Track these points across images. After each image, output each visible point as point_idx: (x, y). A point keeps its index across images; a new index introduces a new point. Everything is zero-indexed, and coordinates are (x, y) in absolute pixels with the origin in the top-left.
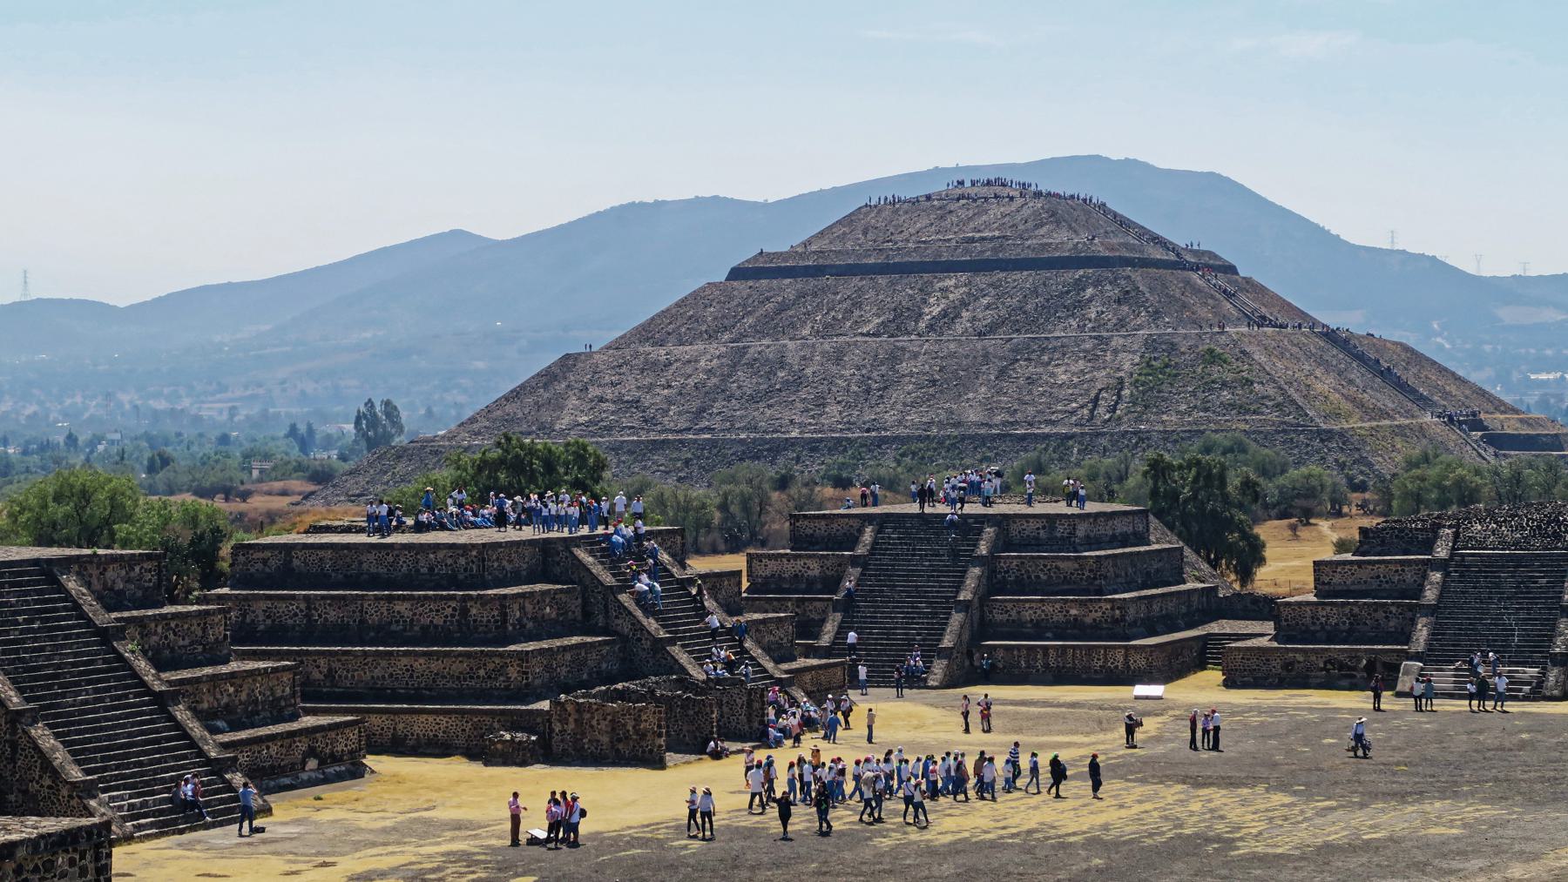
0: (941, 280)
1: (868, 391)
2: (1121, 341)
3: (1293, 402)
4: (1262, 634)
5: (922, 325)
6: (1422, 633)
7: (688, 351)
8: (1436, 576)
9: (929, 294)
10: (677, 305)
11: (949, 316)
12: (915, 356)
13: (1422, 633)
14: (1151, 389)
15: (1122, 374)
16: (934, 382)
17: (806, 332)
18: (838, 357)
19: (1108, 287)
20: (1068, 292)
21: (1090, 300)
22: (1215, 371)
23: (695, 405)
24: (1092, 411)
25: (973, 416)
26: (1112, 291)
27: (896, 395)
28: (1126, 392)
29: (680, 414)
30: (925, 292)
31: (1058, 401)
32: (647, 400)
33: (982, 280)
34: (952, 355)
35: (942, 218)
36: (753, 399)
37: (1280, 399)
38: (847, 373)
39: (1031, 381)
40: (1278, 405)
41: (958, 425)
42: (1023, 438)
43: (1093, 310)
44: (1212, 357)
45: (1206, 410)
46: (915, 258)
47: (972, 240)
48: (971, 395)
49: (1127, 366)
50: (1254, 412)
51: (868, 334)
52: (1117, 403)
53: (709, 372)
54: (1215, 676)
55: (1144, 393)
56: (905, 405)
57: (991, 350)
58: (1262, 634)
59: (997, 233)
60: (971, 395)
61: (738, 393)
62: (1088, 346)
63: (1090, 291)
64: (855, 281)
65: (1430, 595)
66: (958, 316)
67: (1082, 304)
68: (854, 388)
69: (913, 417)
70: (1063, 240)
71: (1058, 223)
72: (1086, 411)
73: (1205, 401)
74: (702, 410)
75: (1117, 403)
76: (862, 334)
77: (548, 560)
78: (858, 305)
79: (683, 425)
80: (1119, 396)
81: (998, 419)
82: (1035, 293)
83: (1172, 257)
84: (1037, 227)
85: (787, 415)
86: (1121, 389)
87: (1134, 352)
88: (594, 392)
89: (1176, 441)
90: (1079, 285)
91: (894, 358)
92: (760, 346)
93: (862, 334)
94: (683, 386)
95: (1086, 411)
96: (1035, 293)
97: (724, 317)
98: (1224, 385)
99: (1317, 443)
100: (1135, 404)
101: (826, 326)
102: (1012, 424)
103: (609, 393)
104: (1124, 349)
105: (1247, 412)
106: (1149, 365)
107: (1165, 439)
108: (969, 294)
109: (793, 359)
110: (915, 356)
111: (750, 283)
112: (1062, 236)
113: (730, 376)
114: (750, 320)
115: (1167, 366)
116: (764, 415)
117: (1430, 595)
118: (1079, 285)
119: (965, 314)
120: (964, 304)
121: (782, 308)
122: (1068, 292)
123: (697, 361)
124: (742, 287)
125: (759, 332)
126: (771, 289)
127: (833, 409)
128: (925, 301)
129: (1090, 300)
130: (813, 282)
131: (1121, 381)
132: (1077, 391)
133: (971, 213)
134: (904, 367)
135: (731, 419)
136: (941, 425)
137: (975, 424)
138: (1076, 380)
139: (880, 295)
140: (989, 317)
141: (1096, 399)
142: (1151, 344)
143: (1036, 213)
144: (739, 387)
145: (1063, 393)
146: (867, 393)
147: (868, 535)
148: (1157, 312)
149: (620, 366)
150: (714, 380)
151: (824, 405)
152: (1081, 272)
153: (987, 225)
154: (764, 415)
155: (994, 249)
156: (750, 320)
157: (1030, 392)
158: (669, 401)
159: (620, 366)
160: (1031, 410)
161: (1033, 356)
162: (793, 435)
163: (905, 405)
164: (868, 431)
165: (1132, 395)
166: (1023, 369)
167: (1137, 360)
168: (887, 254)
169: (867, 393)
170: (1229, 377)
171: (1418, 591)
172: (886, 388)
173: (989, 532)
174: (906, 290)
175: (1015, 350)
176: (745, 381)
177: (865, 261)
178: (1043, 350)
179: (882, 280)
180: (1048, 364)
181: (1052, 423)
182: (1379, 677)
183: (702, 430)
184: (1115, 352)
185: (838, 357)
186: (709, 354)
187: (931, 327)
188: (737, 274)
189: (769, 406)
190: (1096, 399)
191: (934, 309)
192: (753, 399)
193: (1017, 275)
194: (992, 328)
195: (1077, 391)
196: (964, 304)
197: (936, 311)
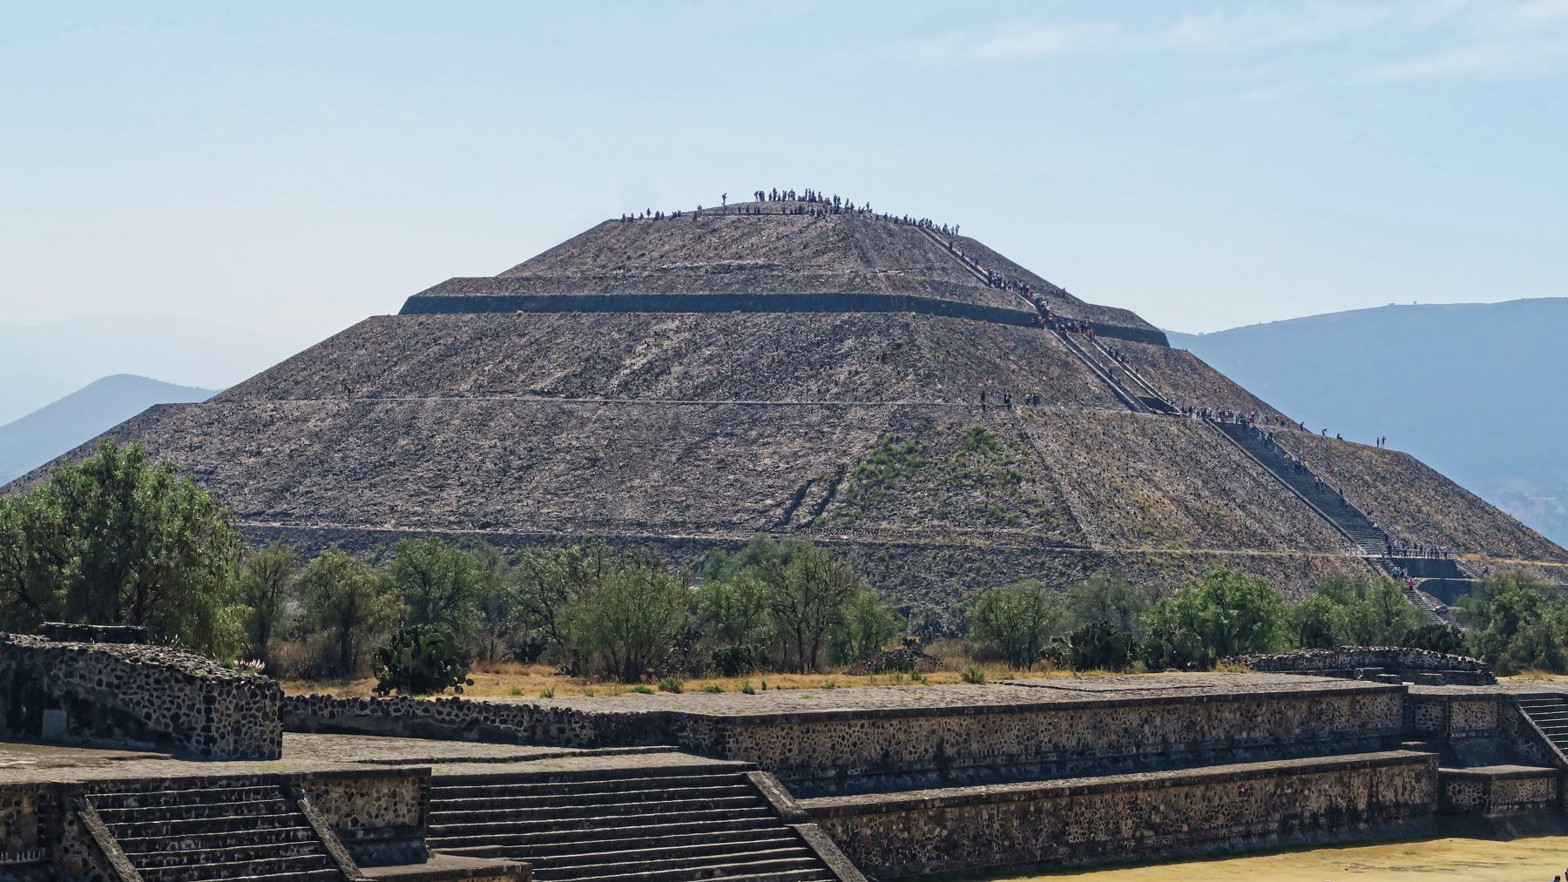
0: (661, 320)
1: (504, 471)
2: (861, 413)
3: (1067, 510)
9: (638, 340)
10: (324, 345)
11: (653, 372)
12: (583, 423)
14: (879, 483)
15: (846, 460)
16: (594, 461)
17: (465, 386)
18: (481, 423)
19: (876, 338)
20: (818, 344)
21: (845, 355)
22: (977, 463)
23: (282, 479)
24: (788, 512)
26: (878, 344)
27: (540, 478)
28: (844, 486)
29: (257, 491)
31: (749, 494)
32: (225, 470)
33: (713, 323)
34: (633, 424)
35: (700, 239)
36: (355, 476)
37: (1050, 506)
38: (486, 444)
39: (722, 465)
40: (1047, 515)
41: (608, 522)
42: (680, 544)
43: (846, 368)
44: (980, 440)
45: (944, 516)
46: (641, 291)
47: (727, 269)
48: (637, 482)
49: (856, 450)
50: (1010, 523)
51: (541, 393)
52: (826, 501)
53: (316, 435)
55: (867, 488)
56: (546, 491)
57: (685, 420)
59: (760, 262)
60: (637, 482)
61: (339, 466)
62: (814, 419)
63: (849, 343)
64: (553, 319)
66: (666, 371)
67: (832, 361)
68: (489, 466)
69: (553, 510)
70: (843, 271)
71: (846, 249)
72: (779, 511)
73: (946, 504)
74: (286, 488)
75: (826, 501)
76: (535, 393)
78: (543, 352)
79: (252, 508)
80: (832, 492)
81: (659, 518)
82: (777, 344)
83: (1029, 307)
84: (817, 253)
85: (391, 499)
86: (839, 481)
87: (873, 430)
89: (882, 560)
90: (838, 334)
91: (554, 425)
92: (395, 406)
93: (535, 393)
94: (276, 453)
95: (779, 511)
97: (373, 363)
98: (981, 480)
99: (1076, 572)
100: (850, 504)
101: (495, 379)
102: (674, 524)
104: (863, 425)
105: (999, 521)
106: (887, 449)
107: (869, 556)
108: (689, 342)
109: (424, 423)
110: (583, 423)
111: (423, 318)
112: (847, 268)
113: (338, 442)
114: (403, 368)
115: (910, 451)
116: (356, 499)
118: (838, 334)
119: (677, 369)
120: (678, 355)
121: (452, 351)
122: (818, 344)
123: (306, 420)
124: (412, 321)
125: (407, 384)
126: (446, 326)
127: (452, 494)
128: (629, 350)
129: (845, 355)
130: (500, 318)
131: (842, 470)
132: (779, 482)
133: (738, 234)
134: (562, 439)
135: (317, 502)
136: (582, 523)
137: (631, 524)
138: (782, 466)
139: (575, 336)
140: (703, 374)
141: (801, 493)
142: (898, 421)
143: (823, 236)
144: (343, 459)
145: (758, 485)
146: (508, 472)
148: (928, 376)
149: (210, 424)
150: (317, 447)
151: (442, 488)
152: (845, 316)
153: (753, 250)
154: (356, 499)
155: (746, 282)
156: (403, 368)
157: (716, 482)
158: (251, 474)
159: (210, 424)
160: (709, 507)
161: (739, 430)
162: (387, 527)
163: (546, 491)
164: (484, 526)
165: (850, 490)
166: (722, 447)
167: (873, 440)
168: (609, 285)
169: (508, 472)
170: (988, 469)
172: (530, 467)
174: (614, 329)
175: (718, 422)
176: (356, 450)
177: (576, 293)
178: (754, 422)
179: (586, 319)
180: (754, 441)
181: (729, 526)
183: (275, 517)
184: (849, 427)
185: (481, 423)
186: (323, 412)
187: (625, 386)
188: (415, 305)
189: (372, 486)
190: (801, 493)
192: (355, 476)
193: (761, 318)
194: (703, 391)
195: (779, 482)
197: (640, 362)
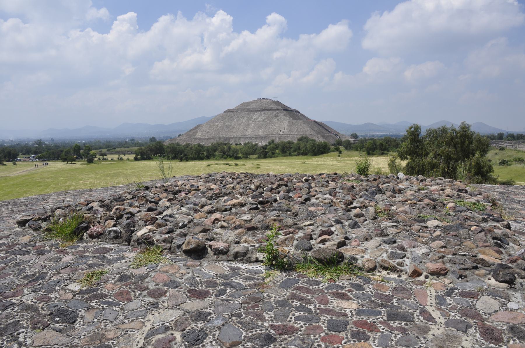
7: (216, 124)
25: (261, 133)
33: (262, 113)
70: (275, 106)
90: (278, 113)
91: (248, 125)
118: (278, 113)
124: (225, 114)
188: (225, 112)
191: (255, 117)
196: (260, 116)
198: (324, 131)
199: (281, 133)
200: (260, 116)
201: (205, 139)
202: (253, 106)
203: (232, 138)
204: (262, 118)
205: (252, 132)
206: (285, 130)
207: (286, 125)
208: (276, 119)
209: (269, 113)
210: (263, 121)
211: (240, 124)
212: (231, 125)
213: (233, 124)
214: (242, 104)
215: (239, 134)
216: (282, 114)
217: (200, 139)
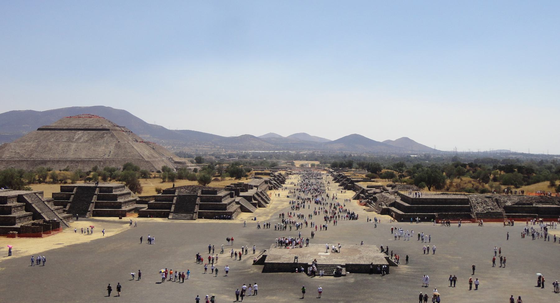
4: (145, 207)
5: (74, 140)
6: (173, 208)
7: (29, 143)
8: (175, 198)
13: (173, 208)
25: (83, 156)
30: (75, 133)
33: (85, 132)
39: (94, 150)
54: (137, 215)
58: (145, 207)
65: (174, 202)
77: (20, 198)
88: (10, 150)
91: (68, 146)
96: (95, 135)
103: (13, 151)
117: (174, 202)
118: (104, 134)
127: (57, 155)
140: (86, 139)
147: (75, 190)
171: (172, 201)
173: (97, 189)
182: (165, 215)
188: (39, 129)
196: (82, 136)
198: (156, 155)
199: (106, 157)
200: (82, 136)
201: (15, 161)
202: (74, 123)
203: (49, 161)
204: (85, 138)
205: (73, 154)
206: (112, 153)
207: (112, 147)
208: (100, 141)
209: (94, 132)
210: (87, 141)
211: (58, 145)
212: (47, 146)
213: (49, 144)
214: (61, 120)
215: (57, 157)
216: (109, 135)
217: (8, 162)
